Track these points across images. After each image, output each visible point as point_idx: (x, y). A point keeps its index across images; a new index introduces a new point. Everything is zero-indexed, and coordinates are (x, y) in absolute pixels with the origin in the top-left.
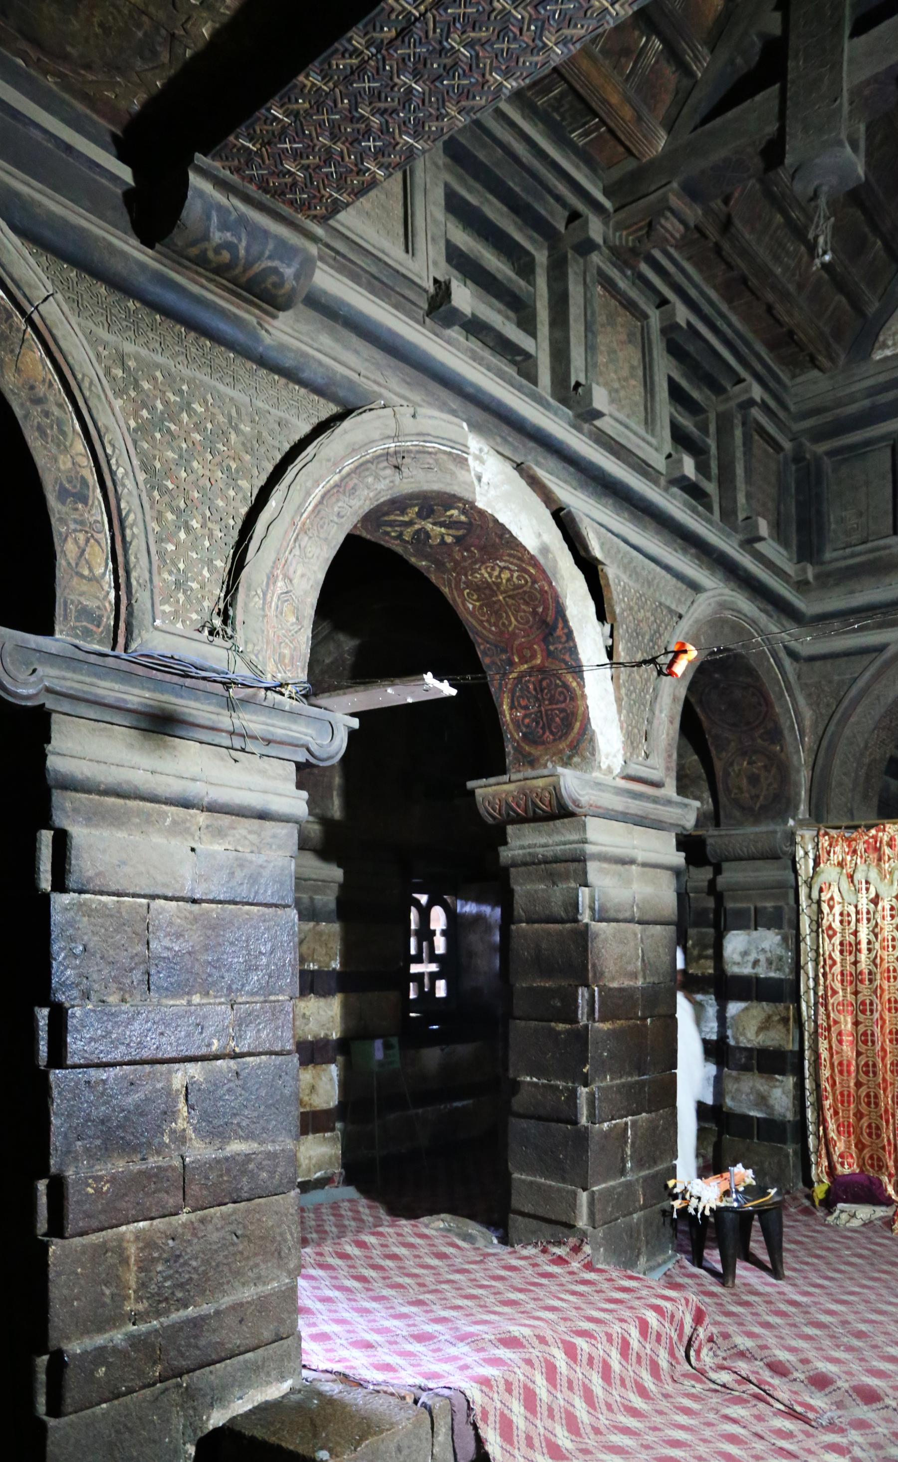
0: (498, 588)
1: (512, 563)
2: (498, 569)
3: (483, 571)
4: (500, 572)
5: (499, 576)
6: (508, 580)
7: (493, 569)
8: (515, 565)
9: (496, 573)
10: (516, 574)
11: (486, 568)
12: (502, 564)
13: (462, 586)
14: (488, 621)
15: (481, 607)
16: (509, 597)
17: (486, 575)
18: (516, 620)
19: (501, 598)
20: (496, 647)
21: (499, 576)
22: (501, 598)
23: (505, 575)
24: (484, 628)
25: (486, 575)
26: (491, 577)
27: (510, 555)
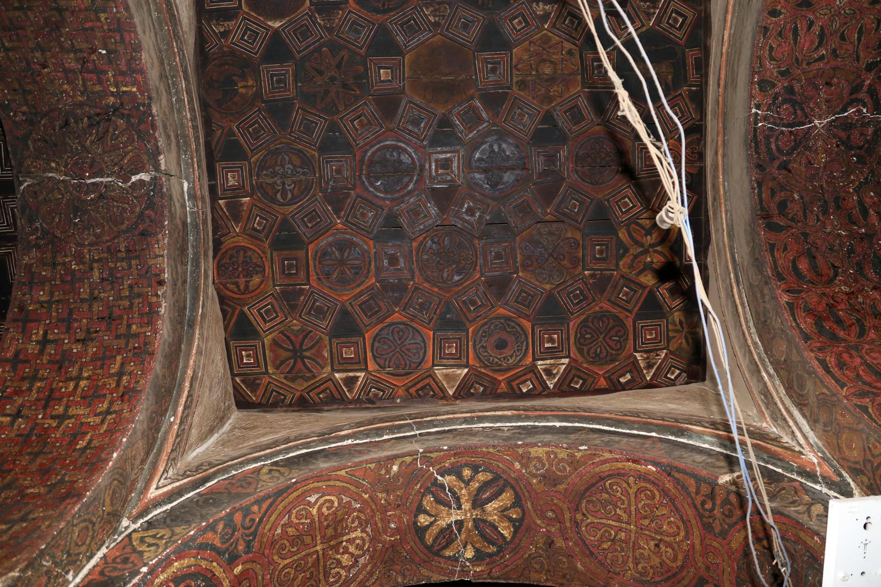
0: (331, 548)
1: (359, 572)
2: (357, 552)
3: (358, 533)
4: (352, 555)
5: (346, 550)
6: (339, 562)
7: (358, 547)
8: (356, 576)
9: (352, 549)
10: (343, 573)
11: (363, 539)
12: (362, 561)
13: (345, 499)
14: (289, 524)
15: (309, 515)
16: (318, 558)
17: (353, 535)
18: (285, 567)
19: (318, 548)
20: (254, 534)
21: (346, 550)
22: (318, 548)
23: (345, 559)
24: (281, 516)
25: (353, 535)
26: (348, 541)
27: (371, 574)
